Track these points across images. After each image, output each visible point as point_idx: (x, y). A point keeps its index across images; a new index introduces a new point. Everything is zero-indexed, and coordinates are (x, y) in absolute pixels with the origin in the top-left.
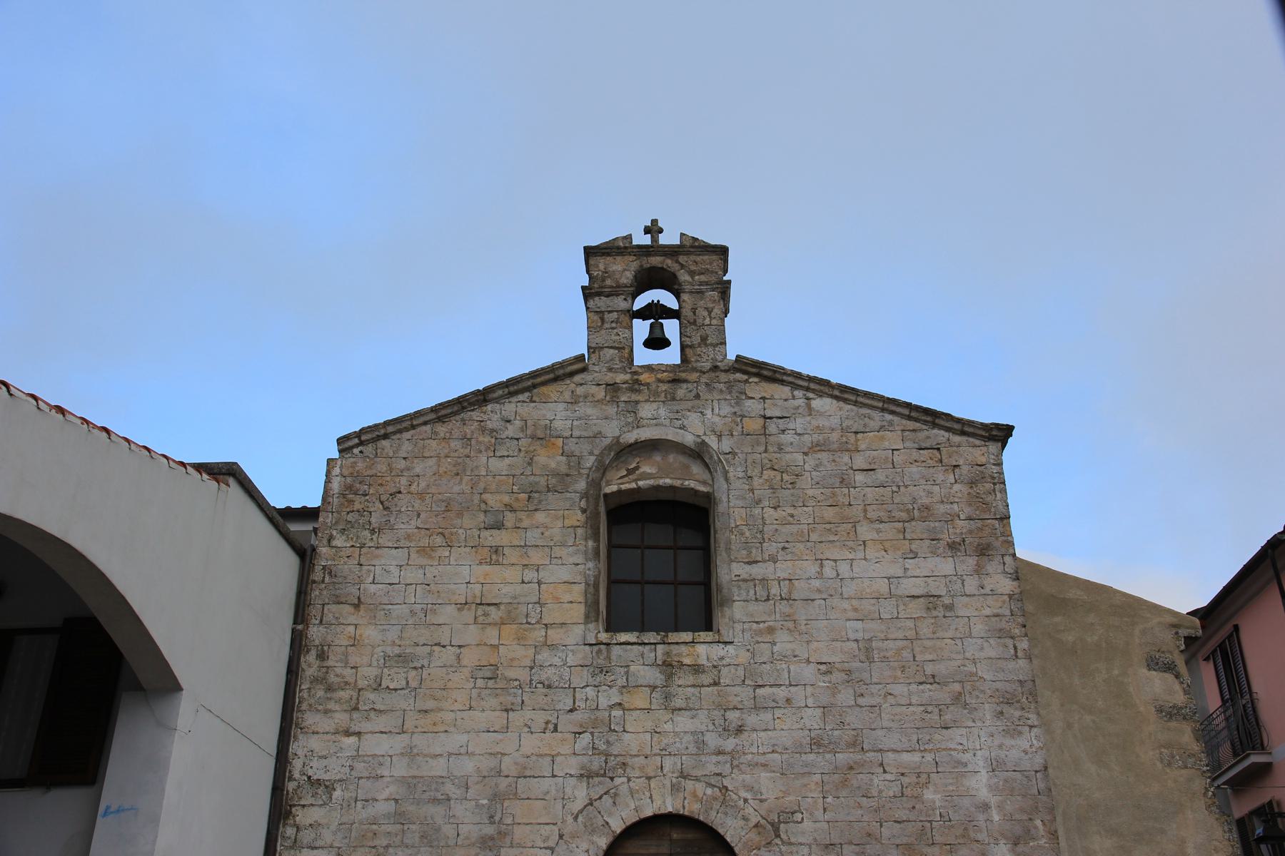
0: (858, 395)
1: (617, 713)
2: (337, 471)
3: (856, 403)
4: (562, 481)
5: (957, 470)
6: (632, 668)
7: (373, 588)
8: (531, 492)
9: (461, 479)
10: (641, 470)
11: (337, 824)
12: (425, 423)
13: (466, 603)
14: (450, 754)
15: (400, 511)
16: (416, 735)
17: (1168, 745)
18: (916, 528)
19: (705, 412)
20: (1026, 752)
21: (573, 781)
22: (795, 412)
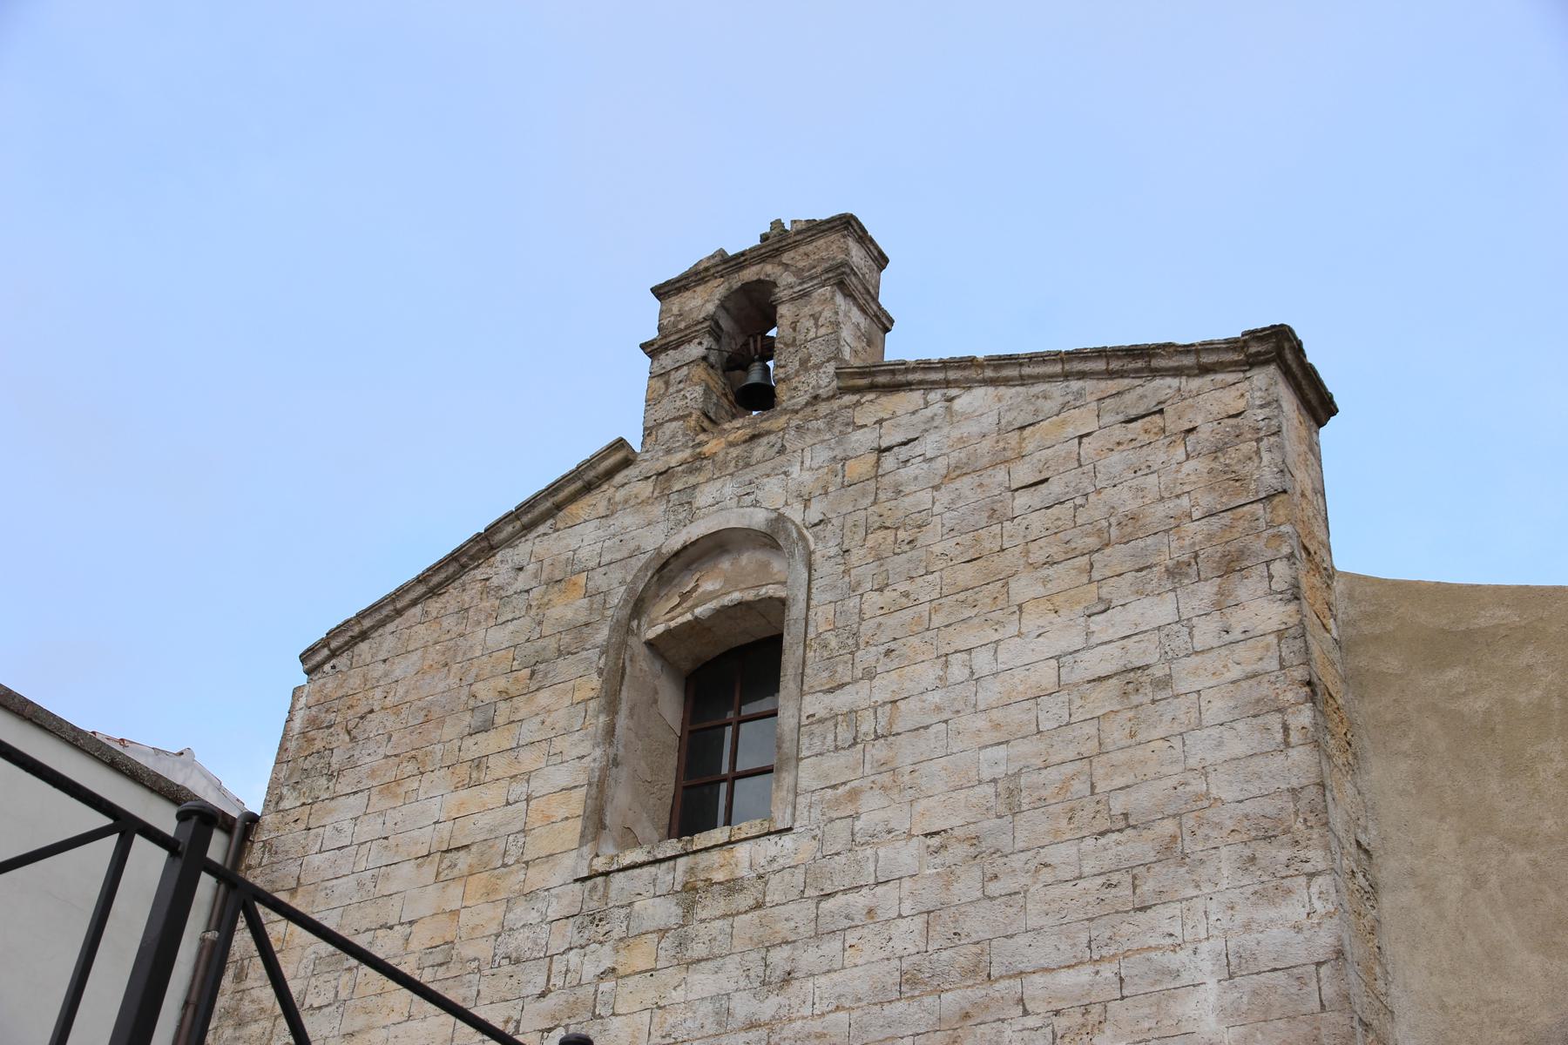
0: (1021, 365)
2: (303, 701)
3: (1023, 380)
5: (1192, 437)
7: (317, 860)
12: (414, 603)
18: (1117, 556)
19: (791, 469)
20: (1298, 928)
22: (927, 426)
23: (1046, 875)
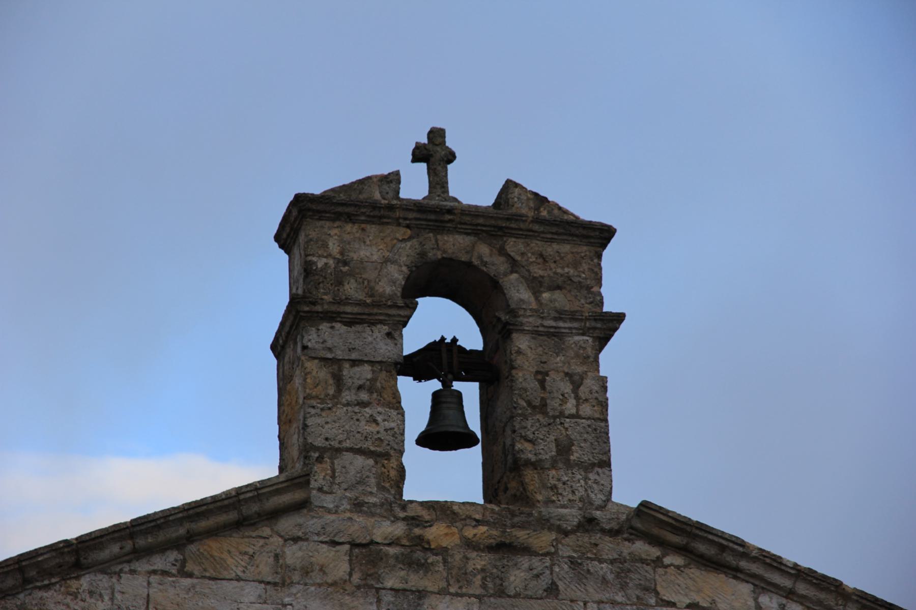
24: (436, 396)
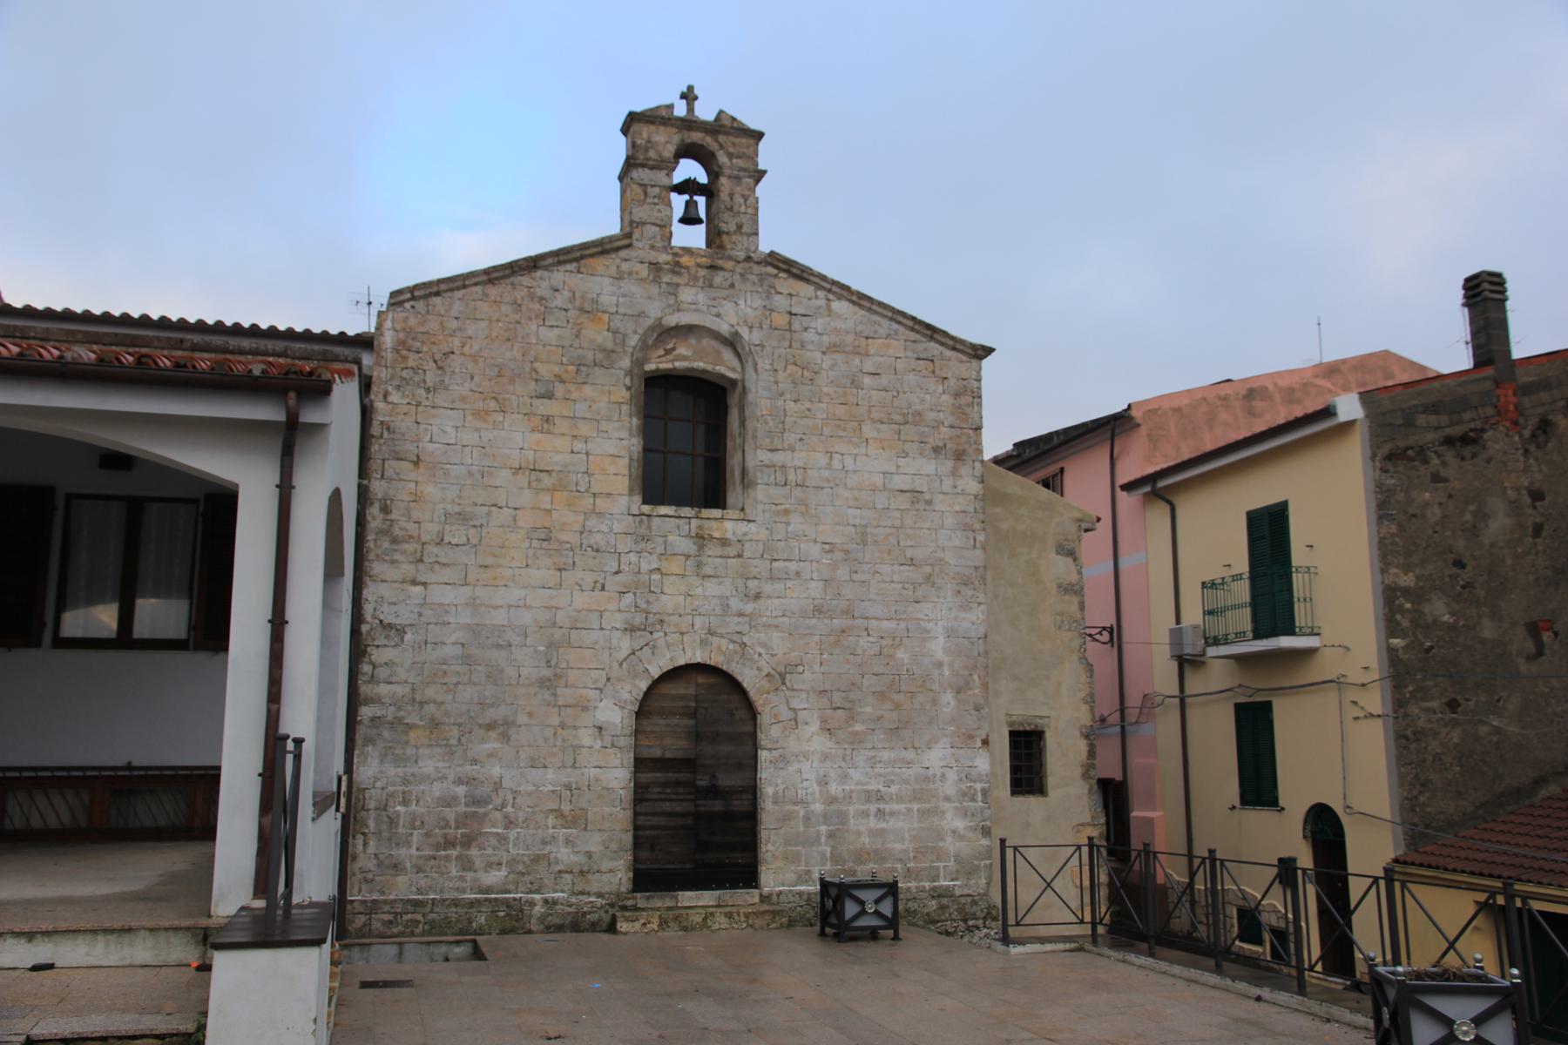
1: (656, 577)
3: (869, 310)
4: (607, 357)
5: (946, 382)
6: (670, 538)
7: (431, 447)
8: (580, 365)
9: (513, 346)
10: (677, 352)
11: (409, 662)
12: (476, 284)
13: (520, 468)
14: (510, 606)
15: (453, 372)
16: (478, 588)
17: (1061, 614)
18: (909, 431)
20: (973, 623)
21: (618, 634)
23: (878, 577)
24: (687, 203)
